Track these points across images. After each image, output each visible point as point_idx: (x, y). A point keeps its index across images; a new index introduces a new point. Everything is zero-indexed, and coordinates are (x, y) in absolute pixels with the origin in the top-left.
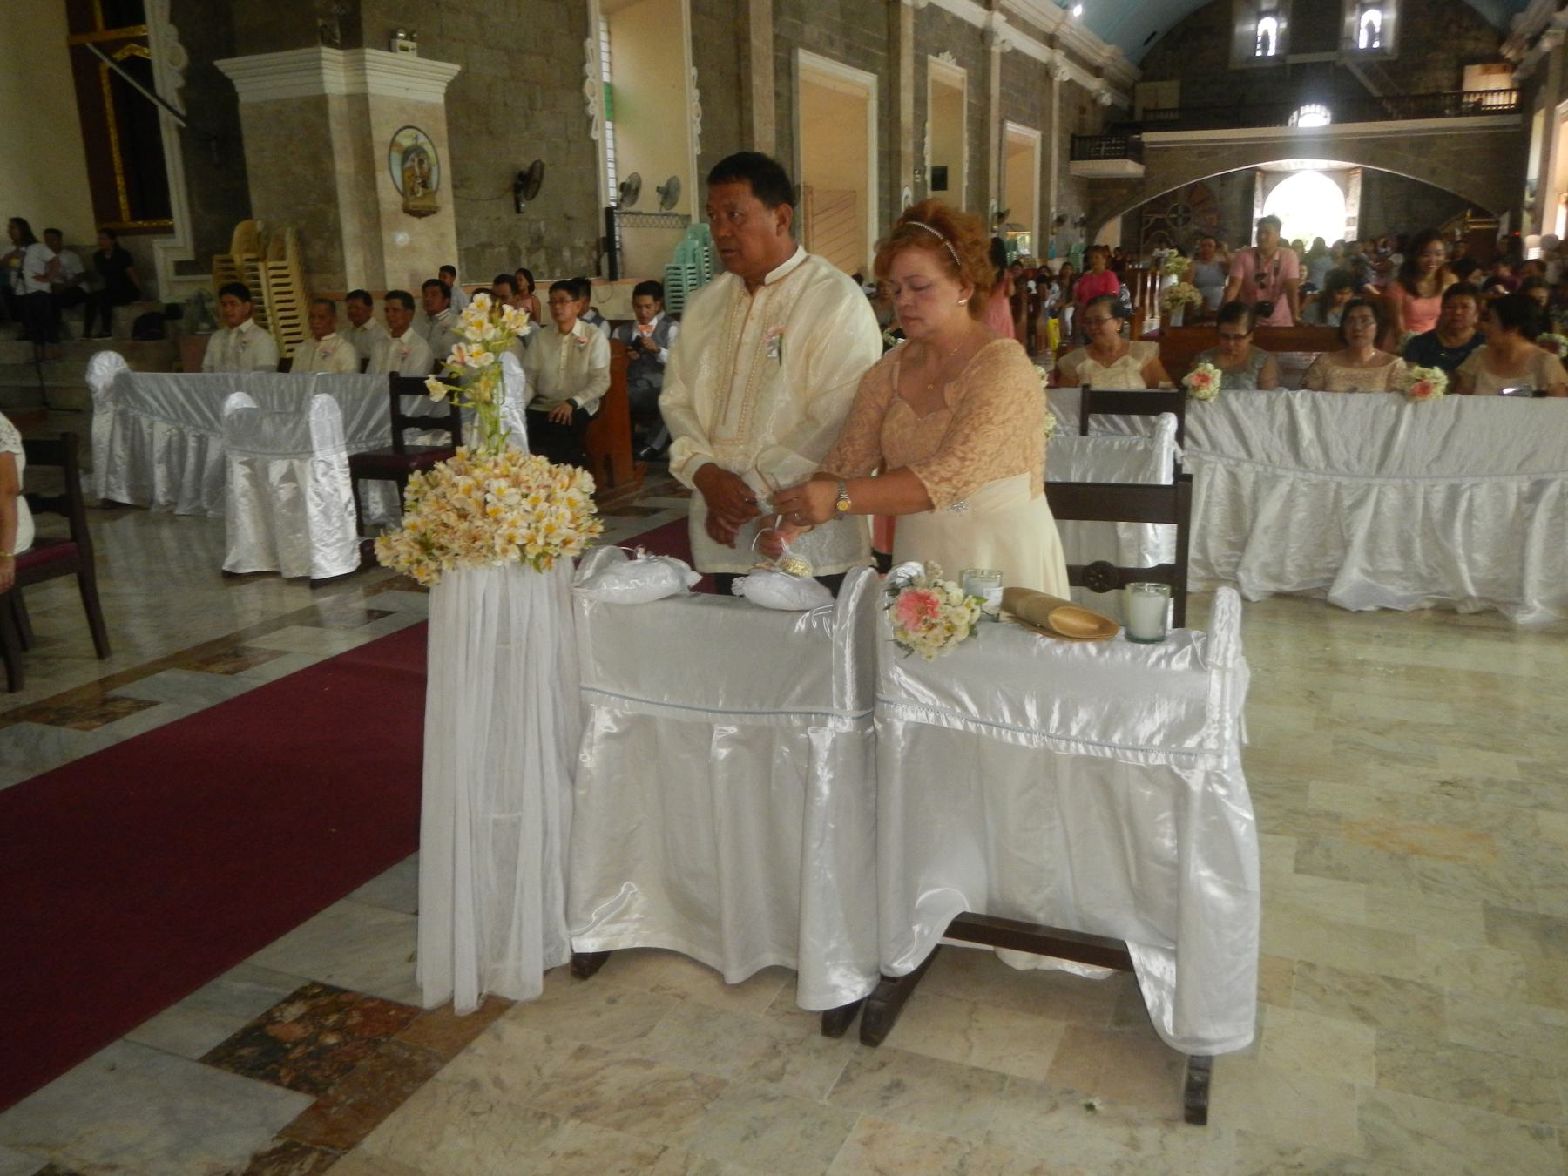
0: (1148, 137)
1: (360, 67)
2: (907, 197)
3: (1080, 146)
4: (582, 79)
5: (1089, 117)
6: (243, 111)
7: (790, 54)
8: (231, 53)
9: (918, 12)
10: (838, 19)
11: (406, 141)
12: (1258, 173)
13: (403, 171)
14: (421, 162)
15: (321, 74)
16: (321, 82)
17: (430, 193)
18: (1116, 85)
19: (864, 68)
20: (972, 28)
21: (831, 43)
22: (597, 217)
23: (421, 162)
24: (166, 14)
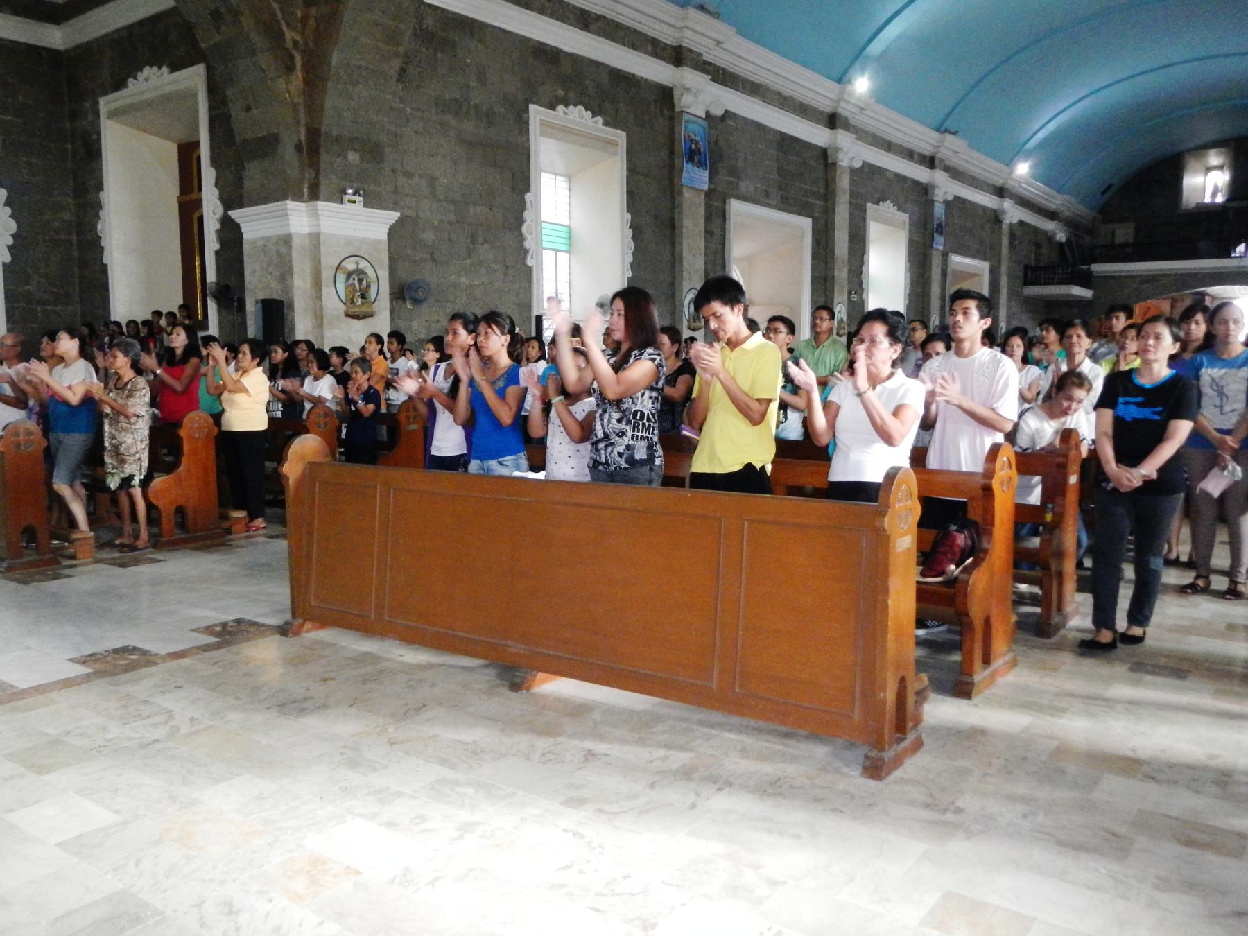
0: (1097, 268)
1: (315, 214)
2: (840, 312)
3: (1032, 274)
4: (520, 221)
5: (1044, 251)
6: (246, 246)
7: (725, 203)
8: (241, 206)
9: (853, 171)
10: (776, 177)
11: (350, 265)
12: (1207, 298)
13: (346, 287)
14: (360, 281)
15: (288, 219)
16: (288, 225)
17: (368, 302)
18: (1072, 224)
19: (800, 214)
20: (916, 183)
21: (767, 195)
22: (530, 322)
23: (360, 281)
24: (213, 181)
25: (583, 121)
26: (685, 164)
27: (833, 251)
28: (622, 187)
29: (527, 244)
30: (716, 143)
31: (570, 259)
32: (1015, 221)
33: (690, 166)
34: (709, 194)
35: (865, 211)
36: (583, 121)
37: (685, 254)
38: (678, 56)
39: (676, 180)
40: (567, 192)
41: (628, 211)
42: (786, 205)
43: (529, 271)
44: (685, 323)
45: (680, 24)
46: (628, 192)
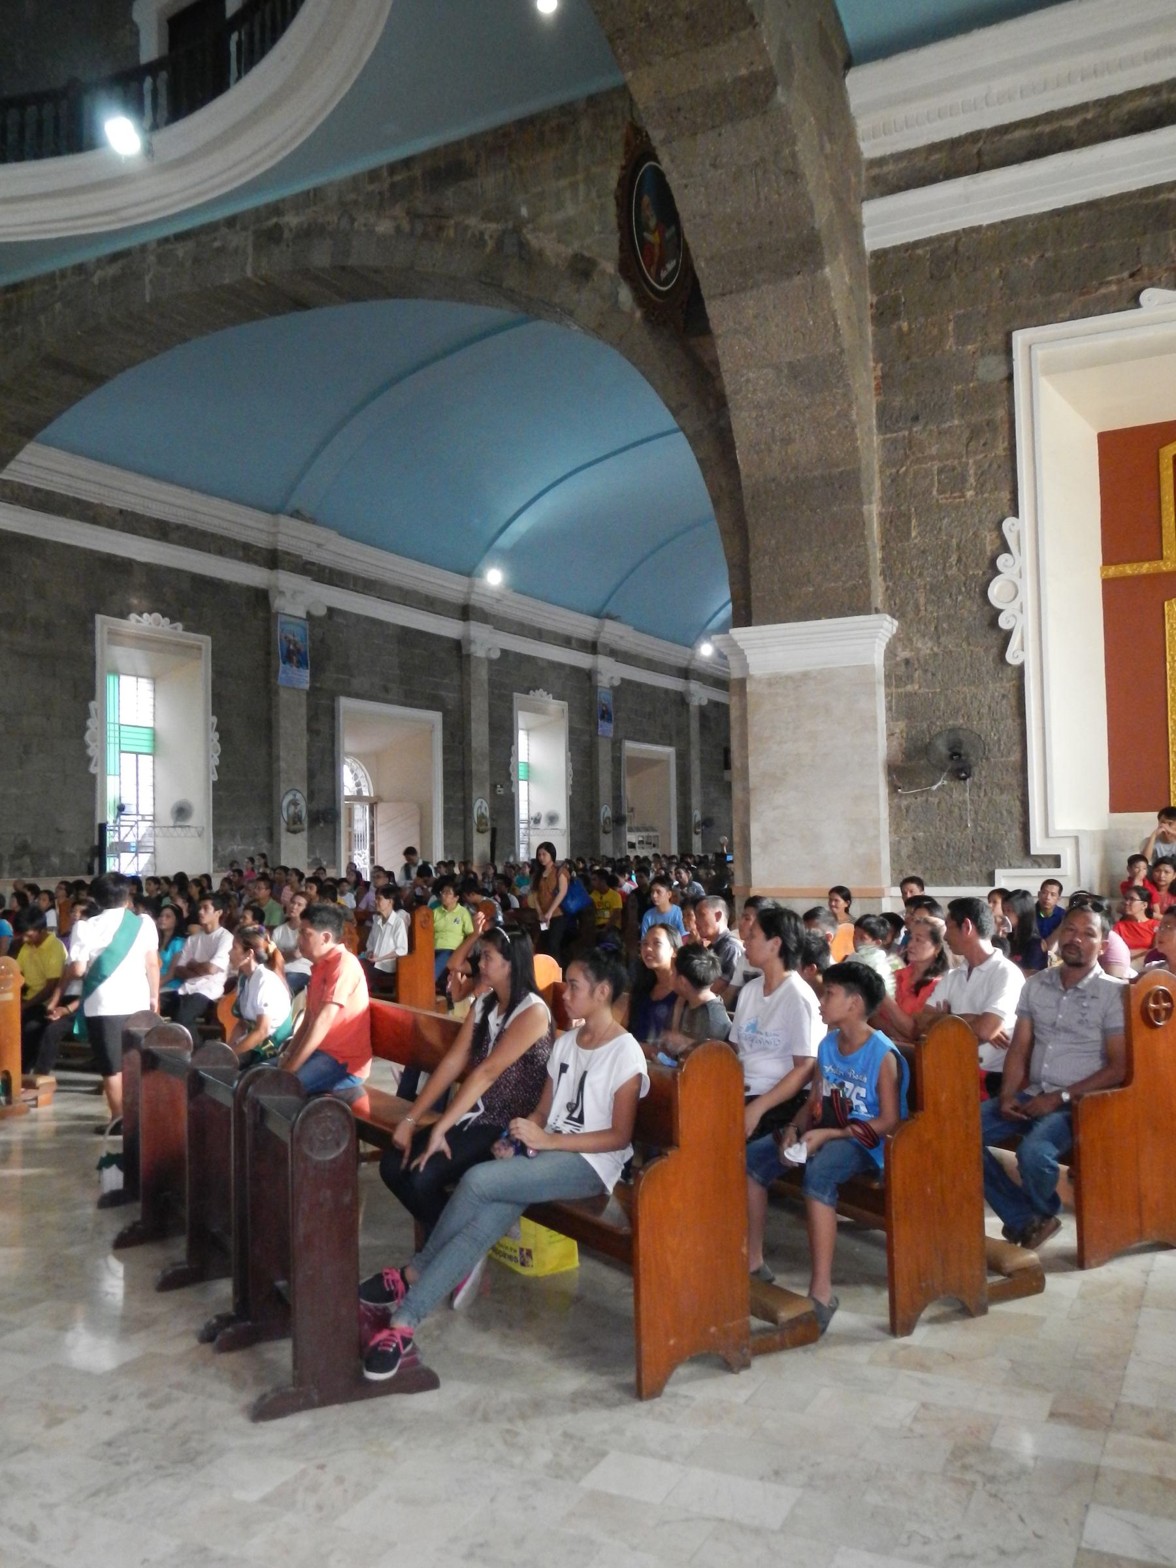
4: (84, 729)
7: (333, 701)
19: (428, 708)
20: (576, 670)
22: (93, 831)
25: (160, 627)
26: (281, 665)
27: (469, 745)
28: (207, 692)
29: (90, 752)
30: (322, 641)
31: (154, 762)
32: (705, 702)
33: (288, 666)
34: (313, 692)
35: (511, 701)
36: (160, 627)
37: (283, 754)
38: (273, 559)
39: (273, 680)
40: (151, 694)
41: (213, 714)
42: (409, 700)
43: (94, 777)
44: (283, 825)
45: (273, 530)
46: (214, 695)
